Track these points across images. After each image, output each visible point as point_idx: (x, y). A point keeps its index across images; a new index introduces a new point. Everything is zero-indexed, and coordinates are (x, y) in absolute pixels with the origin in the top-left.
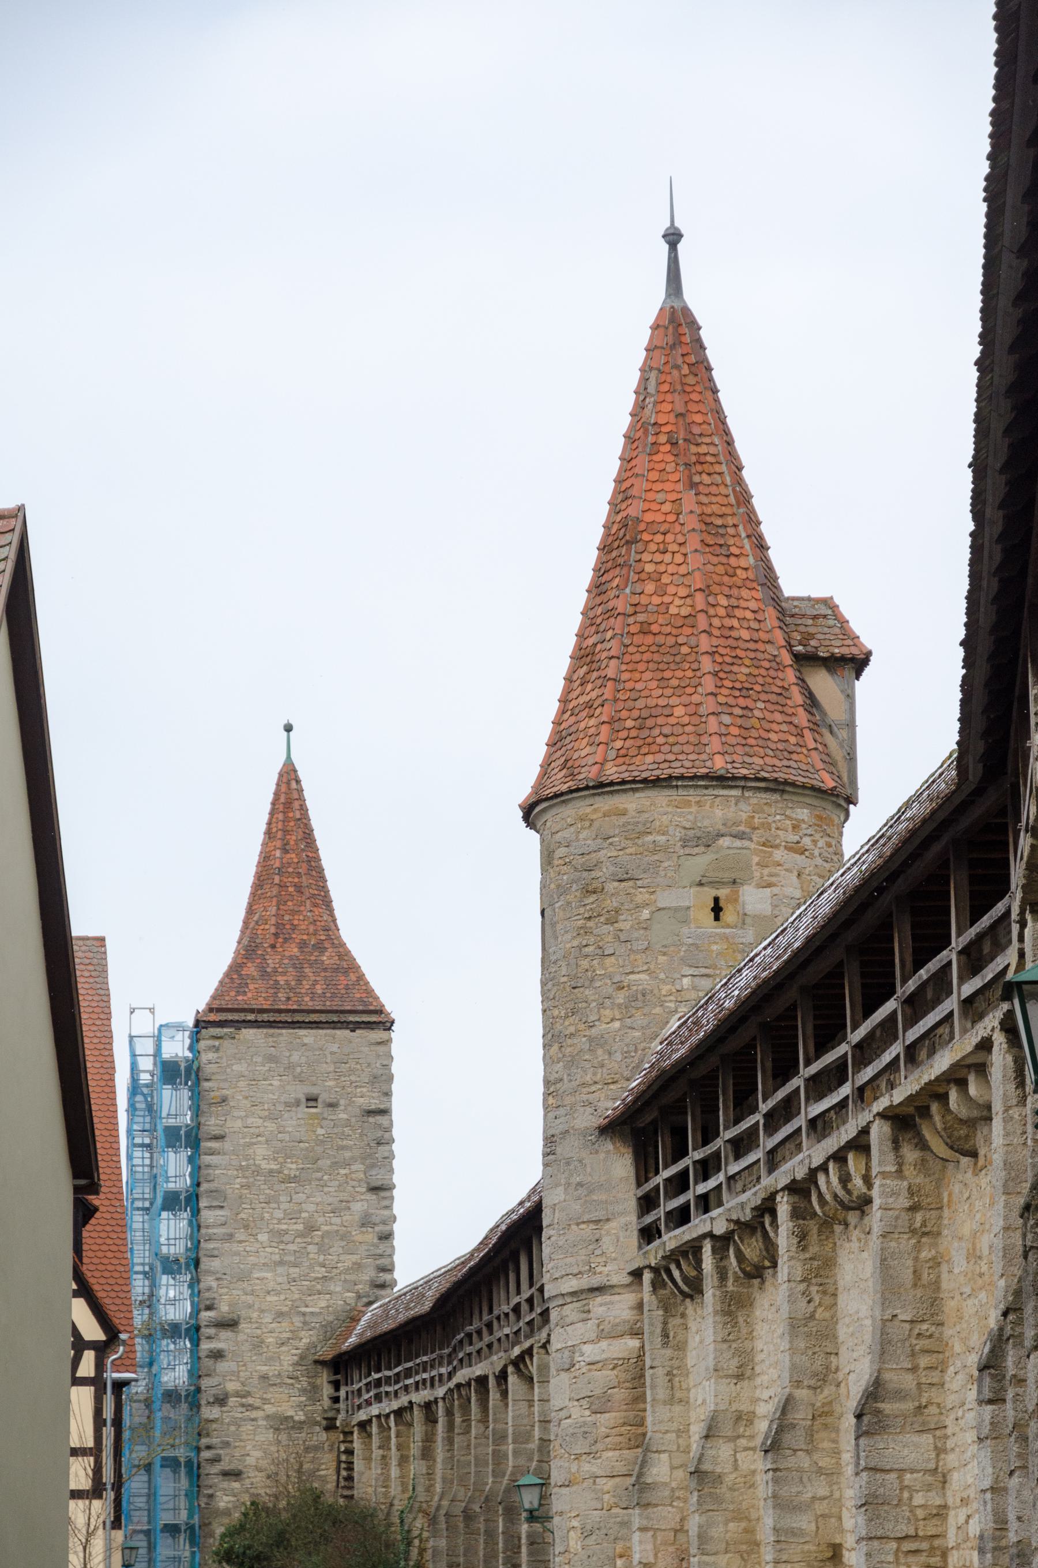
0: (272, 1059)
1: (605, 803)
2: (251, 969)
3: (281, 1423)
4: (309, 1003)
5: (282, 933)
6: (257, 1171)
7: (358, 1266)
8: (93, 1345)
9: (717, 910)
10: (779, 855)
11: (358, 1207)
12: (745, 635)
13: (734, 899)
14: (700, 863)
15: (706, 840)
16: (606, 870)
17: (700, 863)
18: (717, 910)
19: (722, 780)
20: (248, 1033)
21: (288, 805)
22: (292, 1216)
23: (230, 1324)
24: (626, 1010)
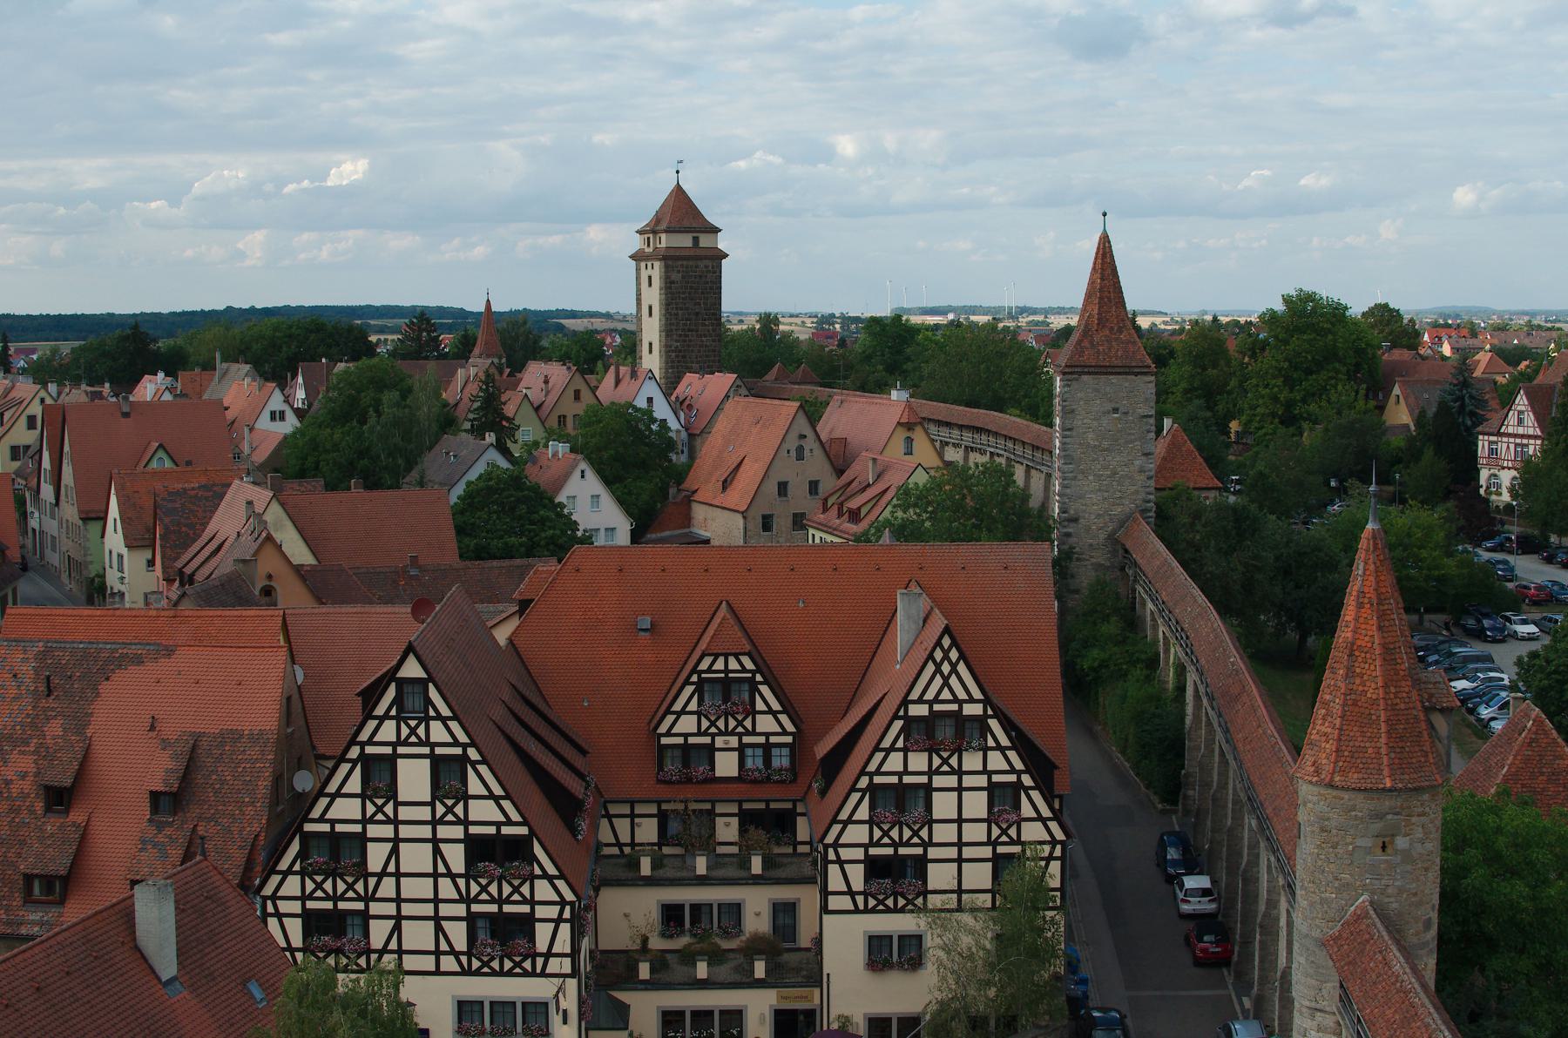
0: (1097, 390)
1: (1335, 793)
2: (1086, 344)
3: (1098, 567)
4: (1116, 363)
5: (1102, 322)
6: (1089, 445)
7: (1137, 492)
8: (1060, 842)
9: (1384, 847)
10: (1414, 819)
11: (1137, 462)
12: (1403, 706)
13: (1392, 843)
14: (1377, 826)
15: (1380, 816)
16: (1334, 823)
17: (1377, 826)
18: (1384, 847)
19: (1390, 790)
20: (1085, 378)
21: (1104, 255)
22: (1105, 468)
23: (1075, 520)
24: (1339, 891)
